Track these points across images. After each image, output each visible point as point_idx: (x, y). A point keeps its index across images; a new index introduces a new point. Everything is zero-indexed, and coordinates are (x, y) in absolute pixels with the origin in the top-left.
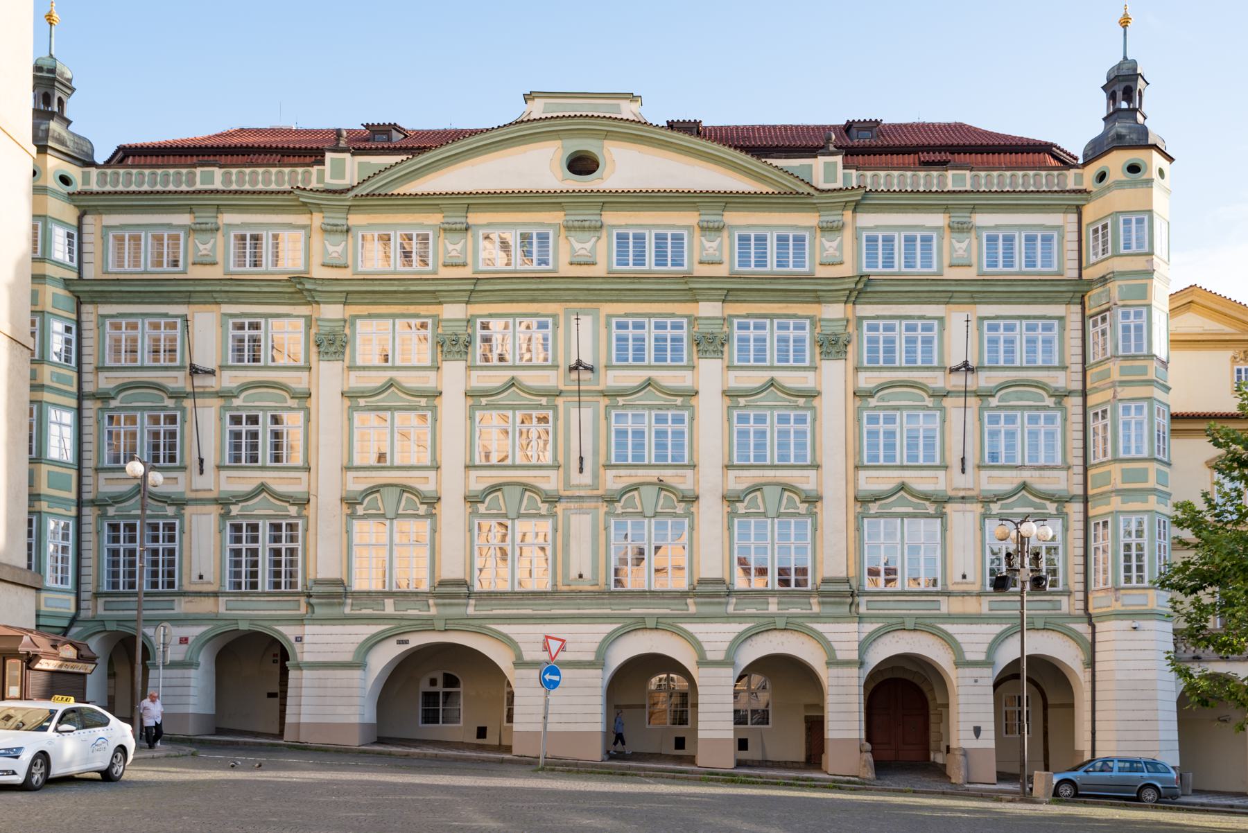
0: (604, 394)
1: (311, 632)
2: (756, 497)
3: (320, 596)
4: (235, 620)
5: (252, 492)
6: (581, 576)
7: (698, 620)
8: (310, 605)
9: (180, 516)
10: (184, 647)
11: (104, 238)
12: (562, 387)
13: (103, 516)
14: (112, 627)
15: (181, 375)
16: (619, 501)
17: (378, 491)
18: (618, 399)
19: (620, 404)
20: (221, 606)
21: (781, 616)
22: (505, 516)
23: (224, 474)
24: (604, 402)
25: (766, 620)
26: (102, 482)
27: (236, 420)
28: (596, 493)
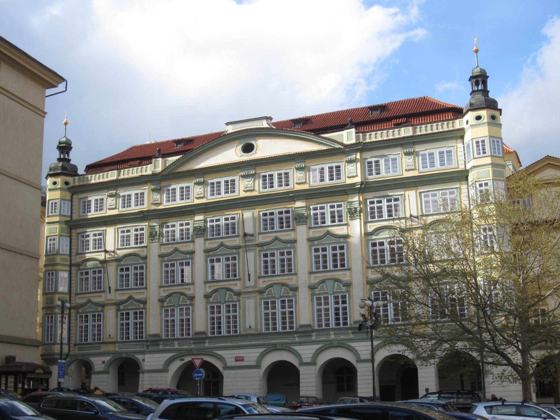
0: (258, 245)
1: (148, 357)
2: (323, 286)
3: (151, 341)
4: (121, 353)
5: (127, 299)
6: (250, 327)
7: (298, 344)
8: (147, 346)
9: (103, 311)
10: (104, 365)
11: (79, 203)
12: (242, 244)
13: (78, 313)
14: (79, 358)
15: (103, 254)
16: (265, 292)
17: (171, 296)
18: (264, 247)
19: (265, 249)
20: (117, 348)
21: (335, 340)
22: (220, 302)
23: (118, 292)
24: (258, 249)
25: (328, 342)
26: (77, 298)
27: (122, 270)
28: (256, 289)
